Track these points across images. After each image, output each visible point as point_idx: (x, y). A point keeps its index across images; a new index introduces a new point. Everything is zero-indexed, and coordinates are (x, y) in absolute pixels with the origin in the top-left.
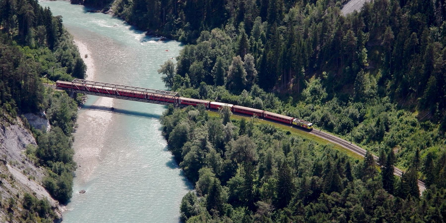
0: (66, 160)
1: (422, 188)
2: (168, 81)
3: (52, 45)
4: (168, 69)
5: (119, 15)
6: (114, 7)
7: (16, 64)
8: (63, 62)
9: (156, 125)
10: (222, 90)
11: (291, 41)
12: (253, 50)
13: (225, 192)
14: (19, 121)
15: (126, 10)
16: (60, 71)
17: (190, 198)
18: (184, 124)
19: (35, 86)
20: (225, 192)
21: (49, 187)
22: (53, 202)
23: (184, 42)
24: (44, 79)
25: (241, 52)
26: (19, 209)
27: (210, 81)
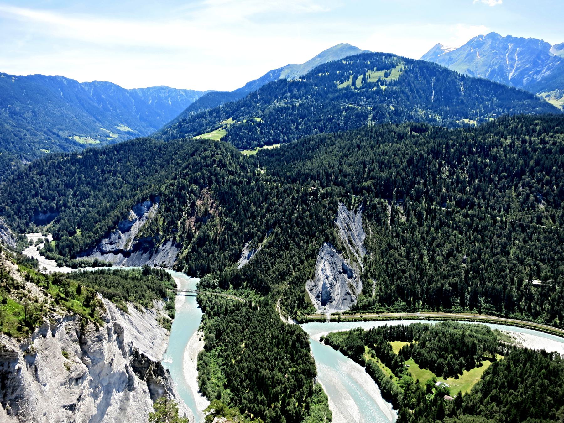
0: (173, 308)
1: (259, 308)
2: (198, 287)
3: (169, 280)
4: (197, 284)
5: (184, 272)
6: (183, 270)
7: (160, 286)
8: (172, 284)
9: (195, 298)
10: (210, 289)
11: (226, 275)
12: (217, 278)
13: (212, 313)
14: (161, 299)
15: (187, 271)
16: (171, 287)
17: (204, 315)
18: (202, 297)
19: (165, 291)
20: (212, 313)
21: (169, 315)
22: (170, 319)
23: (200, 278)
24: (167, 289)
25: (214, 279)
26: (162, 321)
27: (207, 286)
